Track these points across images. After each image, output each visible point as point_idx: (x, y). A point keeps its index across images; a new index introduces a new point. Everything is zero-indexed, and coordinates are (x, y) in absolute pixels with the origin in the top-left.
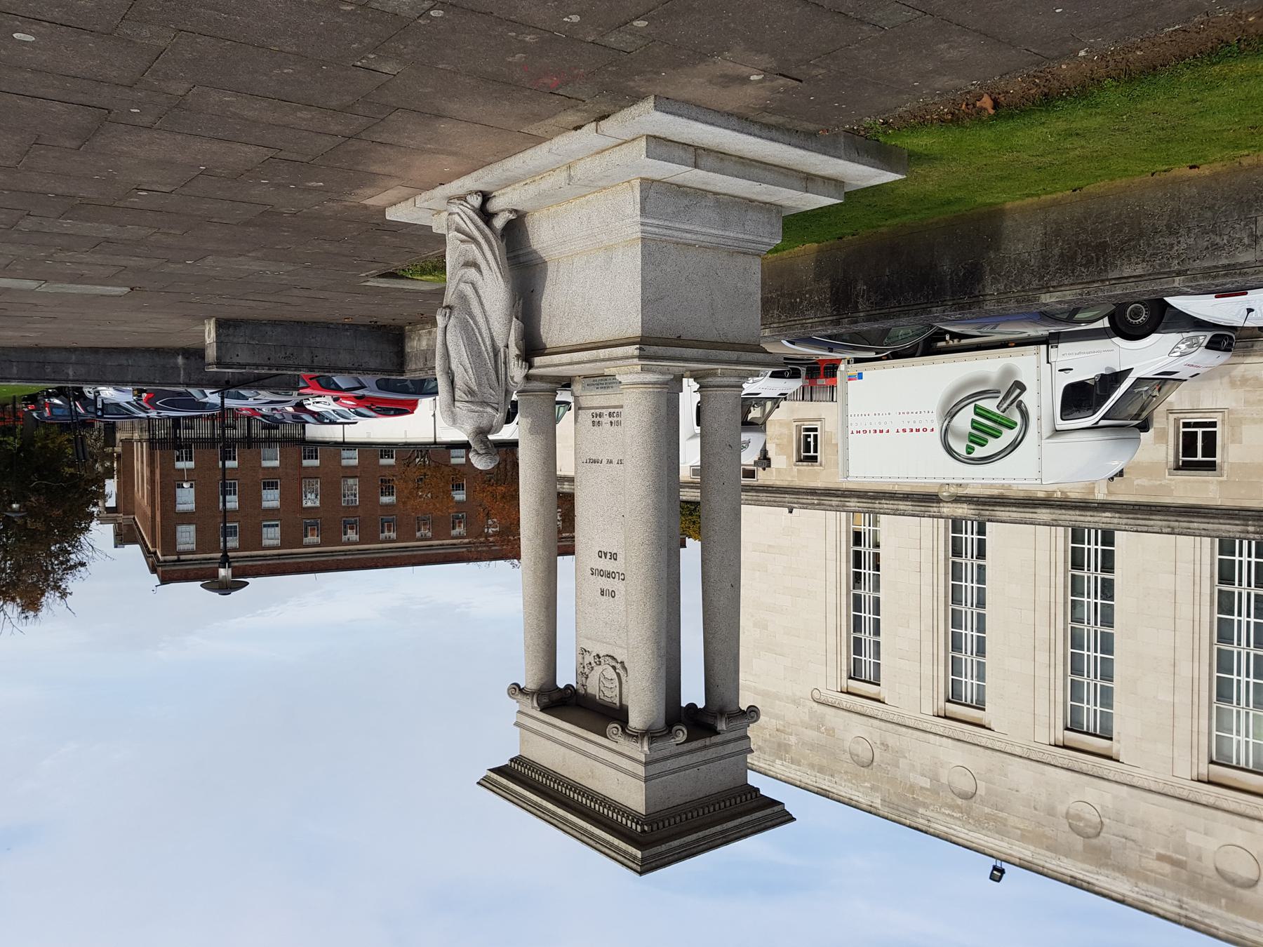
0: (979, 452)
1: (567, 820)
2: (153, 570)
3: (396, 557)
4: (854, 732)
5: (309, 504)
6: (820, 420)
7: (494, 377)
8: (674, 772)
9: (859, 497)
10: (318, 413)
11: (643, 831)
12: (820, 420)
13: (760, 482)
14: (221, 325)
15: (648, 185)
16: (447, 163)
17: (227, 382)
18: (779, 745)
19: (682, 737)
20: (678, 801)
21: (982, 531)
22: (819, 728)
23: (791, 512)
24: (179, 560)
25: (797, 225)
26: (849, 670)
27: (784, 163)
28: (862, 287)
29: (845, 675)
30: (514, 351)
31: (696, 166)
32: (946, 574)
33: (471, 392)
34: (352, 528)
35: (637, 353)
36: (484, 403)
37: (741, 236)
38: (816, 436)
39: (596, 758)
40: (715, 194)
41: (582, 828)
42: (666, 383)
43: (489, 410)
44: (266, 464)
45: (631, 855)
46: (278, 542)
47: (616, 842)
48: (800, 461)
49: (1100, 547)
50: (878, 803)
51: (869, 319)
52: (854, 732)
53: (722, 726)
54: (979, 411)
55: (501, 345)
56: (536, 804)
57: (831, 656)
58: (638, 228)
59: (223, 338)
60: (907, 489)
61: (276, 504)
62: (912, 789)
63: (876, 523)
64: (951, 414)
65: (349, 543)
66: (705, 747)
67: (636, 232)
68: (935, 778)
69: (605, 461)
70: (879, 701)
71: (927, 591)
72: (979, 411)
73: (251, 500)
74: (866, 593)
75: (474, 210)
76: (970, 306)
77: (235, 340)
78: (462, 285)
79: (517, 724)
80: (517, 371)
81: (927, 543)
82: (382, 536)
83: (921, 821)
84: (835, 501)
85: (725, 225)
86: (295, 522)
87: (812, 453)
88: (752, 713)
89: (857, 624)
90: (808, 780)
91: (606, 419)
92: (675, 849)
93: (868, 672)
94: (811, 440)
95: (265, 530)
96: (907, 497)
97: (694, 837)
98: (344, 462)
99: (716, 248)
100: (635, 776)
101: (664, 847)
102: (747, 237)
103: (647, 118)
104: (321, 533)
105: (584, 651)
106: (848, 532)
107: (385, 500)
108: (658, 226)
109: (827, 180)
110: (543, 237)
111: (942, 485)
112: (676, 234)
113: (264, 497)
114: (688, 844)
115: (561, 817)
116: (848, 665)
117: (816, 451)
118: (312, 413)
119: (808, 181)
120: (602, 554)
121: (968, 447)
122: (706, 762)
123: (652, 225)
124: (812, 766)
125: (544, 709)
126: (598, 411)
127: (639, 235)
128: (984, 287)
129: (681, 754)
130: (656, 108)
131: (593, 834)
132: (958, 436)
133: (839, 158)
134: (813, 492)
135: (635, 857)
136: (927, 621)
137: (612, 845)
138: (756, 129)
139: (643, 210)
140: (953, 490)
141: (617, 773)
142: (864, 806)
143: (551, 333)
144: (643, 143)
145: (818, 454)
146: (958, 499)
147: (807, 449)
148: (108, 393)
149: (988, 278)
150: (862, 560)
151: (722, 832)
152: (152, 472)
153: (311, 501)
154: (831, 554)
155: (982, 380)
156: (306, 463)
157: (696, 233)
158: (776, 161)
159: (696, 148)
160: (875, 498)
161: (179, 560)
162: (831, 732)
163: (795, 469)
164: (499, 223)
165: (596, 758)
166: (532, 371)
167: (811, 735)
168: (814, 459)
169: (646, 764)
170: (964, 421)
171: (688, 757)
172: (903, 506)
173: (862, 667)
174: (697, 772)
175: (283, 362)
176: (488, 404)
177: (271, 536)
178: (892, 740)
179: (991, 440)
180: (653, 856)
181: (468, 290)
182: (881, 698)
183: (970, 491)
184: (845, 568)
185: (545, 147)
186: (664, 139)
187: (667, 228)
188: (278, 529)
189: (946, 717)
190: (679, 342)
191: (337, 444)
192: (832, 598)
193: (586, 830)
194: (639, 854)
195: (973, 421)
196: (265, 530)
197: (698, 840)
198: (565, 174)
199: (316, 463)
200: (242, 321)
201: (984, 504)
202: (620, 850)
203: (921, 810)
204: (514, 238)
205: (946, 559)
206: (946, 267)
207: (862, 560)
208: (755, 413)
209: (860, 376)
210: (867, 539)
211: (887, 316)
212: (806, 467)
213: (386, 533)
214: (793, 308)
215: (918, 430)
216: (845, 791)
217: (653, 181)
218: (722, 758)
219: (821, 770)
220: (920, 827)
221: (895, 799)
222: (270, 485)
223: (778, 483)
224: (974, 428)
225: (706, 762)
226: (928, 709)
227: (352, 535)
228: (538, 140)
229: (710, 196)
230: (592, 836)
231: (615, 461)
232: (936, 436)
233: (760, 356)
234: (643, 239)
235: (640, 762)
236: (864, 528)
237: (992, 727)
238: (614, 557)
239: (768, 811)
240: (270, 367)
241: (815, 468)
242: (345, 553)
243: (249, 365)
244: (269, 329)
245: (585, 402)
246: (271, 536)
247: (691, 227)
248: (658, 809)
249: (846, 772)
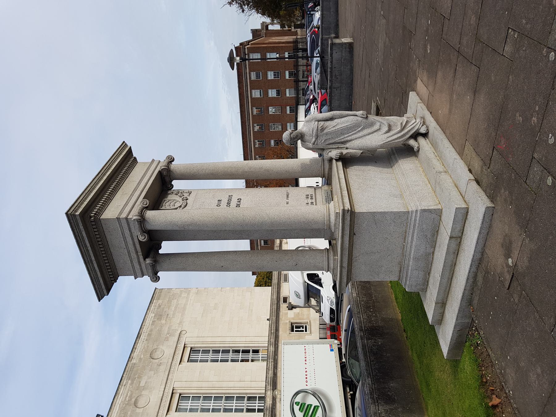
0: (296, 408)
1: (100, 180)
2: (241, 44)
3: (247, 147)
4: (166, 350)
5: (270, 110)
6: (311, 333)
7: (331, 142)
8: (123, 234)
9: (275, 351)
10: (310, 109)
11: (91, 217)
12: (311, 333)
13: (281, 305)
14: (351, 45)
15: (439, 213)
16: (443, 111)
17: (323, 57)
18: (161, 315)
19: (141, 238)
20: (108, 237)
21: (260, 411)
22: (168, 334)
23: (268, 320)
24: (245, 54)
25: (414, 303)
26: (195, 347)
27: (453, 289)
28: (380, 341)
29: (193, 346)
30: (345, 152)
31: (451, 238)
32: (239, 393)
33: (323, 129)
34: (260, 128)
35: (346, 208)
36: (317, 137)
37: (410, 268)
38: (303, 331)
39: (132, 195)
40: (433, 253)
41: (95, 187)
42: (330, 228)
43: (314, 140)
44: (287, 91)
45: (78, 209)
46: (254, 96)
47: (86, 203)
48: (292, 324)
50: (134, 361)
51: (364, 347)
52: (166, 350)
53: (148, 261)
54: (316, 408)
55: (348, 145)
56: (111, 167)
57: (201, 340)
58: (414, 209)
59: (344, 46)
60: (278, 375)
61: (270, 95)
62: (140, 377)
63: (263, 360)
64: (314, 394)
65: (253, 127)
66: (137, 252)
67: (412, 207)
68: (144, 388)
69: (287, 201)
70: (181, 362)
71: (231, 384)
72: (316, 408)
73: (271, 84)
74: (231, 356)
75: (418, 130)
76: (372, 398)
77: (343, 52)
78: (378, 124)
79: (153, 160)
80: (334, 154)
81: (254, 384)
82: (256, 141)
83: (125, 382)
84: (273, 340)
85: (416, 259)
86: (262, 104)
87: (295, 329)
88: (156, 279)
89: (216, 352)
90: (145, 329)
91: (310, 201)
92: (81, 233)
93: (193, 357)
94: (301, 329)
95: (259, 91)
96: (275, 374)
97: (88, 245)
98: (288, 124)
99: (403, 255)
100: (121, 213)
101: (81, 227)
102: (409, 271)
103: (479, 204)
104: (258, 115)
105: (190, 193)
106: (258, 347)
107: (272, 142)
108: (415, 220)
109: (442, 315)
110: (405, 165)
111: (280, 391)
112: (411, 231)
113: (273, 90)
114: (84, 241)
116: (197, 347)
117: (296, 331)
118: (310, 107)
119: (442, 304)
120: (239, 200)
121: (299, 403)
122: (129, 252)
123: (416, 216)
124: (151, 331)
125: (160, 173)
126: (314, 197)
127: (410, 210)
129: (133, 239)
130: (487, 208)
131: (91, 192)
132: (304, 398)
133: (457, 319)
134: (277, 330)
135: (76, 211)
136: (217, 385)
137: (84, 201)
138: (474, 269)
139: (424, 211)
140: (278, 396)
141: (124, 204)
142: (132, 355)
143: (355, 171)
144: (464, 206)
145: (295, 332)
146: (274, 399)
147: (297, 327)
148: (317, 15)
150: (246, 354)
151: (91, 260)
152: (283, 43)
153: (272, 110)
154: (248, 339)
155: (331, 409)
156: (288, 108)
157: (412, 242)
158: (453, 285)
159: (461, 238)
160: (274, 359)
161: (245, 54)
162: (167, 339)
163: (288, 322)
164: (412, 142)
165: (132, 195)
166: (334, 161)
167: (165, 330)
168: (292, 331)
169: (126, 218)
170: (312, 401)
171: (131, 242)
172: (271, 372)
173: (195, 354)
174: (124, 247)
175: (334, 74)
176: (316, 139)
177: (256, 94)
178: (162, 368)
179: (303, 413)
180: (77, 221)
181: (376, 127)
182: (182, 363)
183: (278, 404)
184: (241, 346)
185: (458, 157)
186: (466, 218)
187: (414, 225)
188: (259, 96)
189: (173, 393)
190: (352, 234)
191: (296, 118)
192: (228, 339)
193: (94, 189)
194: (78, 213)
195: (311, 405)
196: (259, 91)
197: (86, 246)
198: (441, 170)
199: (288, 112)
200: (353, 54)
201: (272, 412)
202: (81, 204)
203: (130, 382)
204: (404, 150)
205: (246, 394)
207: (246, 354)
208: (313, 302)
209: (332, 350)
210: (255, 356)
212: (289, 326)
213: (258, 143)
214: (368, 308)
215: (306, 378)
216: (139, 346)
217: (440, 216)
218: (132, 262)
219: (149, 335)
220: (122, 381)
221: (135, 369)
222: (278, 93)
223: (281, 314)
224: (308, 405)
225: (129, 252)
226: (177, 385)
227: (257, 128)
228: (461, 153)
229: (432, 250)
230: (90, 191)
232: (303, 387)
233: (345, 280)
234: (408, 212)
235: (128, 216)
236: (260, 355)
237: (168, 416)
238: (238, 206)
239: (103, 287)
240: (331, 68)
241: (288, 331)
242: (249, 125)
243: (332, 58)
244: (349, 67)
245: (318, 191)
246: (256, 94)
247: (415, 239)
248: (103, 226)
249: (148, 346)
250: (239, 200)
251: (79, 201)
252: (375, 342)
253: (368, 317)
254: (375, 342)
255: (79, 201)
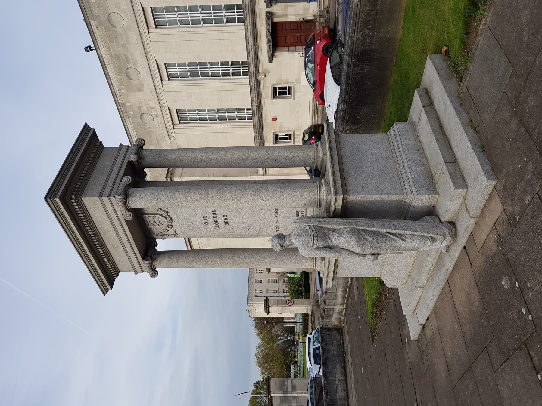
1: (89, 258)
28: (366, 69)
41: (94, 266)
49: (236, 17)
115: (87, 255)
120: (225, 216)
128: (350, 126)
131: (97, 271)
149: (353, 127)
165: (126, 252)
193: (95, 268)
206: (364, 110)
211: (347, 83)
214: (366, 22)
230: (96, 272)
231: (277, 224)
238: (227, 224)
250: (225, 216)
251: (100, 284)
252: (361, 70)
253: (363, 37)
254: (361, 70)
255: (100, 284)
